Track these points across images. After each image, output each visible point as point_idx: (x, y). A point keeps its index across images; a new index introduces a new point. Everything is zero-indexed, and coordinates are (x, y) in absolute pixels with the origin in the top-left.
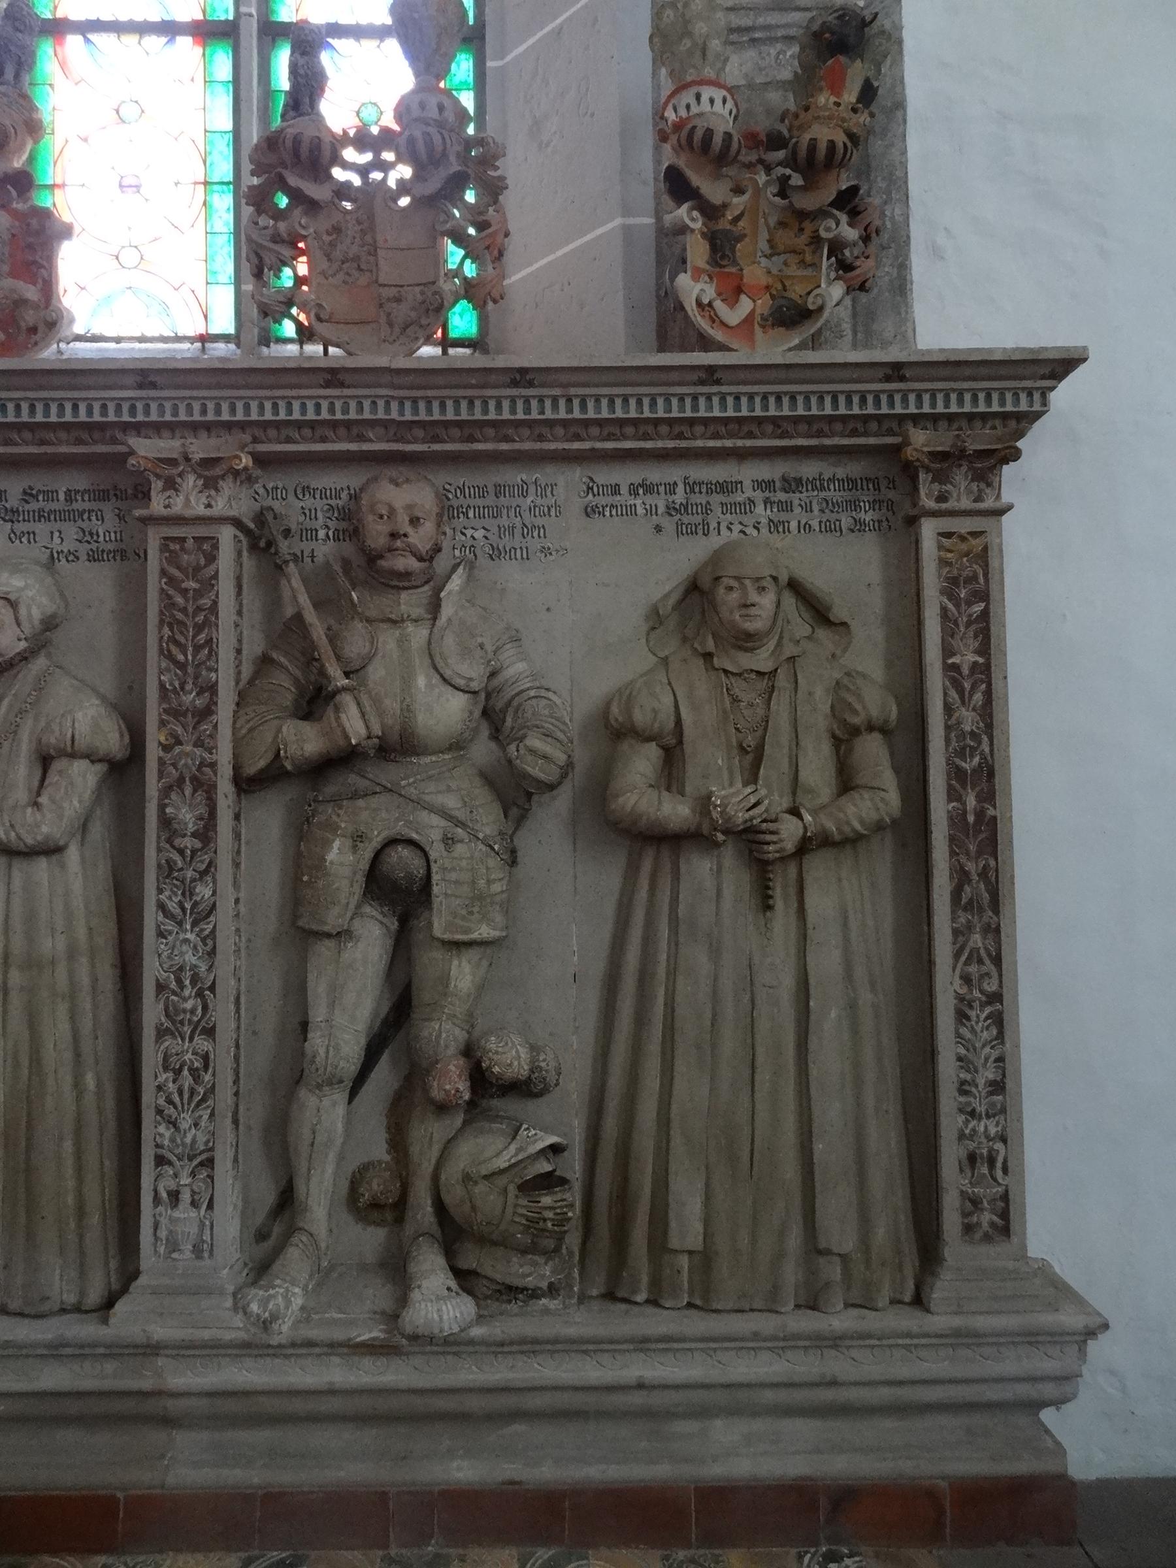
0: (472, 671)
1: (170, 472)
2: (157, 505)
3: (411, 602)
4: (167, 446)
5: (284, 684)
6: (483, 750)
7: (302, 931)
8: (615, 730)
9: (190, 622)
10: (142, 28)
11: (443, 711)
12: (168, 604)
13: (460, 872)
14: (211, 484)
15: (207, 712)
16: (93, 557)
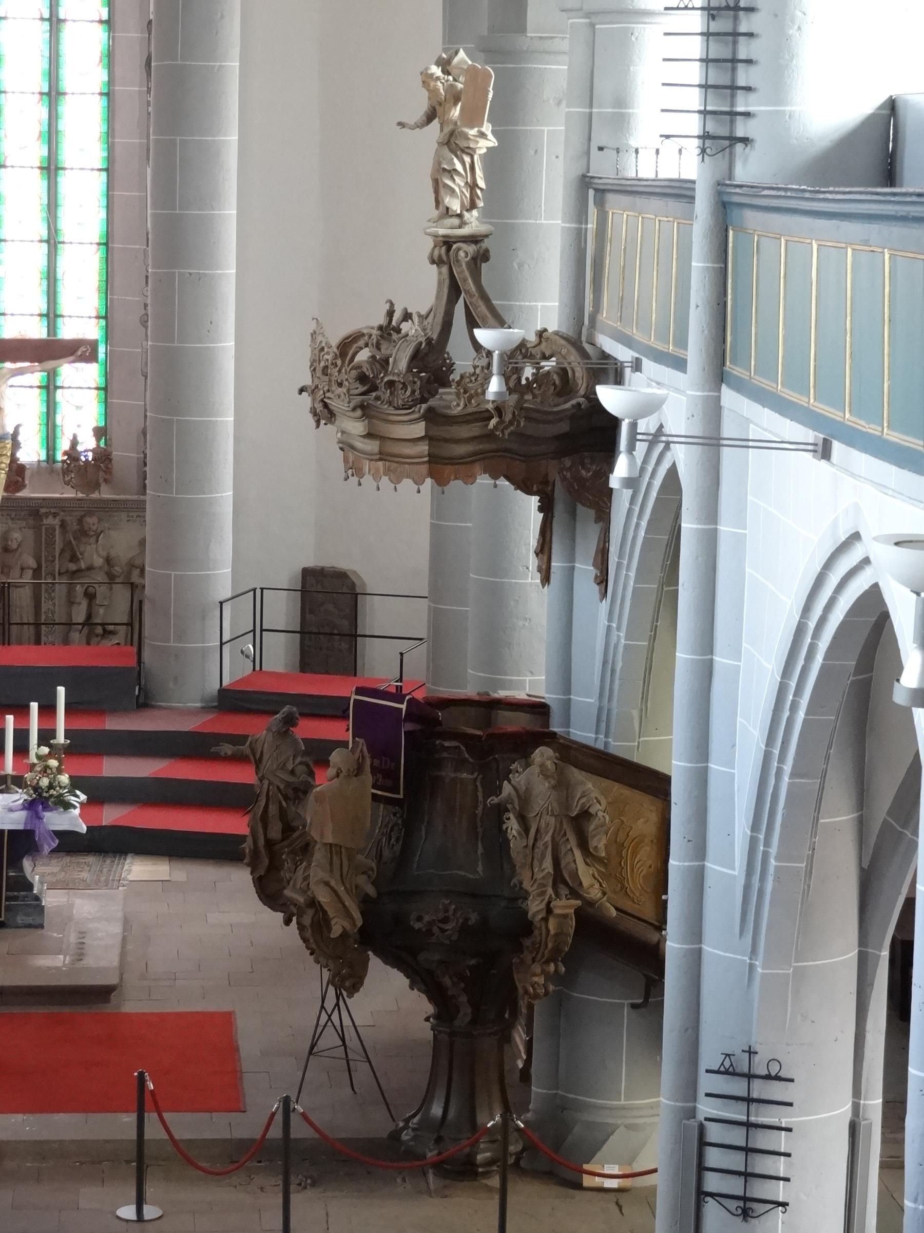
0: (104, 554)
1: (47, 515)
2: (45, 522)
3: (93, 540)
4: (47, 510)
5: (67, 555)
6: (106, 568)
7: (71, 602)
8: (131, 565)
9: (51, 543)
10: (25, 387)
11: (98, 561)
12: (46, 540)
13: (101, 591)
14: (55, 517)
15: (53, 561)
16: (29, 528)
